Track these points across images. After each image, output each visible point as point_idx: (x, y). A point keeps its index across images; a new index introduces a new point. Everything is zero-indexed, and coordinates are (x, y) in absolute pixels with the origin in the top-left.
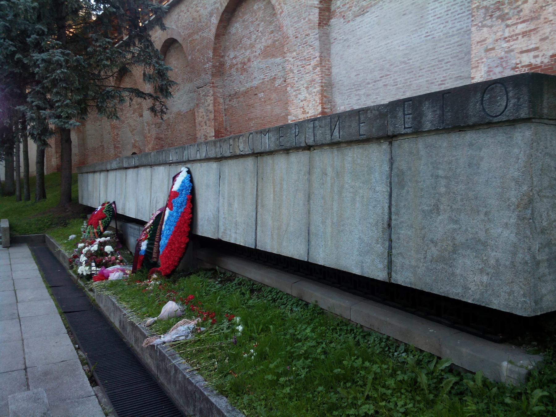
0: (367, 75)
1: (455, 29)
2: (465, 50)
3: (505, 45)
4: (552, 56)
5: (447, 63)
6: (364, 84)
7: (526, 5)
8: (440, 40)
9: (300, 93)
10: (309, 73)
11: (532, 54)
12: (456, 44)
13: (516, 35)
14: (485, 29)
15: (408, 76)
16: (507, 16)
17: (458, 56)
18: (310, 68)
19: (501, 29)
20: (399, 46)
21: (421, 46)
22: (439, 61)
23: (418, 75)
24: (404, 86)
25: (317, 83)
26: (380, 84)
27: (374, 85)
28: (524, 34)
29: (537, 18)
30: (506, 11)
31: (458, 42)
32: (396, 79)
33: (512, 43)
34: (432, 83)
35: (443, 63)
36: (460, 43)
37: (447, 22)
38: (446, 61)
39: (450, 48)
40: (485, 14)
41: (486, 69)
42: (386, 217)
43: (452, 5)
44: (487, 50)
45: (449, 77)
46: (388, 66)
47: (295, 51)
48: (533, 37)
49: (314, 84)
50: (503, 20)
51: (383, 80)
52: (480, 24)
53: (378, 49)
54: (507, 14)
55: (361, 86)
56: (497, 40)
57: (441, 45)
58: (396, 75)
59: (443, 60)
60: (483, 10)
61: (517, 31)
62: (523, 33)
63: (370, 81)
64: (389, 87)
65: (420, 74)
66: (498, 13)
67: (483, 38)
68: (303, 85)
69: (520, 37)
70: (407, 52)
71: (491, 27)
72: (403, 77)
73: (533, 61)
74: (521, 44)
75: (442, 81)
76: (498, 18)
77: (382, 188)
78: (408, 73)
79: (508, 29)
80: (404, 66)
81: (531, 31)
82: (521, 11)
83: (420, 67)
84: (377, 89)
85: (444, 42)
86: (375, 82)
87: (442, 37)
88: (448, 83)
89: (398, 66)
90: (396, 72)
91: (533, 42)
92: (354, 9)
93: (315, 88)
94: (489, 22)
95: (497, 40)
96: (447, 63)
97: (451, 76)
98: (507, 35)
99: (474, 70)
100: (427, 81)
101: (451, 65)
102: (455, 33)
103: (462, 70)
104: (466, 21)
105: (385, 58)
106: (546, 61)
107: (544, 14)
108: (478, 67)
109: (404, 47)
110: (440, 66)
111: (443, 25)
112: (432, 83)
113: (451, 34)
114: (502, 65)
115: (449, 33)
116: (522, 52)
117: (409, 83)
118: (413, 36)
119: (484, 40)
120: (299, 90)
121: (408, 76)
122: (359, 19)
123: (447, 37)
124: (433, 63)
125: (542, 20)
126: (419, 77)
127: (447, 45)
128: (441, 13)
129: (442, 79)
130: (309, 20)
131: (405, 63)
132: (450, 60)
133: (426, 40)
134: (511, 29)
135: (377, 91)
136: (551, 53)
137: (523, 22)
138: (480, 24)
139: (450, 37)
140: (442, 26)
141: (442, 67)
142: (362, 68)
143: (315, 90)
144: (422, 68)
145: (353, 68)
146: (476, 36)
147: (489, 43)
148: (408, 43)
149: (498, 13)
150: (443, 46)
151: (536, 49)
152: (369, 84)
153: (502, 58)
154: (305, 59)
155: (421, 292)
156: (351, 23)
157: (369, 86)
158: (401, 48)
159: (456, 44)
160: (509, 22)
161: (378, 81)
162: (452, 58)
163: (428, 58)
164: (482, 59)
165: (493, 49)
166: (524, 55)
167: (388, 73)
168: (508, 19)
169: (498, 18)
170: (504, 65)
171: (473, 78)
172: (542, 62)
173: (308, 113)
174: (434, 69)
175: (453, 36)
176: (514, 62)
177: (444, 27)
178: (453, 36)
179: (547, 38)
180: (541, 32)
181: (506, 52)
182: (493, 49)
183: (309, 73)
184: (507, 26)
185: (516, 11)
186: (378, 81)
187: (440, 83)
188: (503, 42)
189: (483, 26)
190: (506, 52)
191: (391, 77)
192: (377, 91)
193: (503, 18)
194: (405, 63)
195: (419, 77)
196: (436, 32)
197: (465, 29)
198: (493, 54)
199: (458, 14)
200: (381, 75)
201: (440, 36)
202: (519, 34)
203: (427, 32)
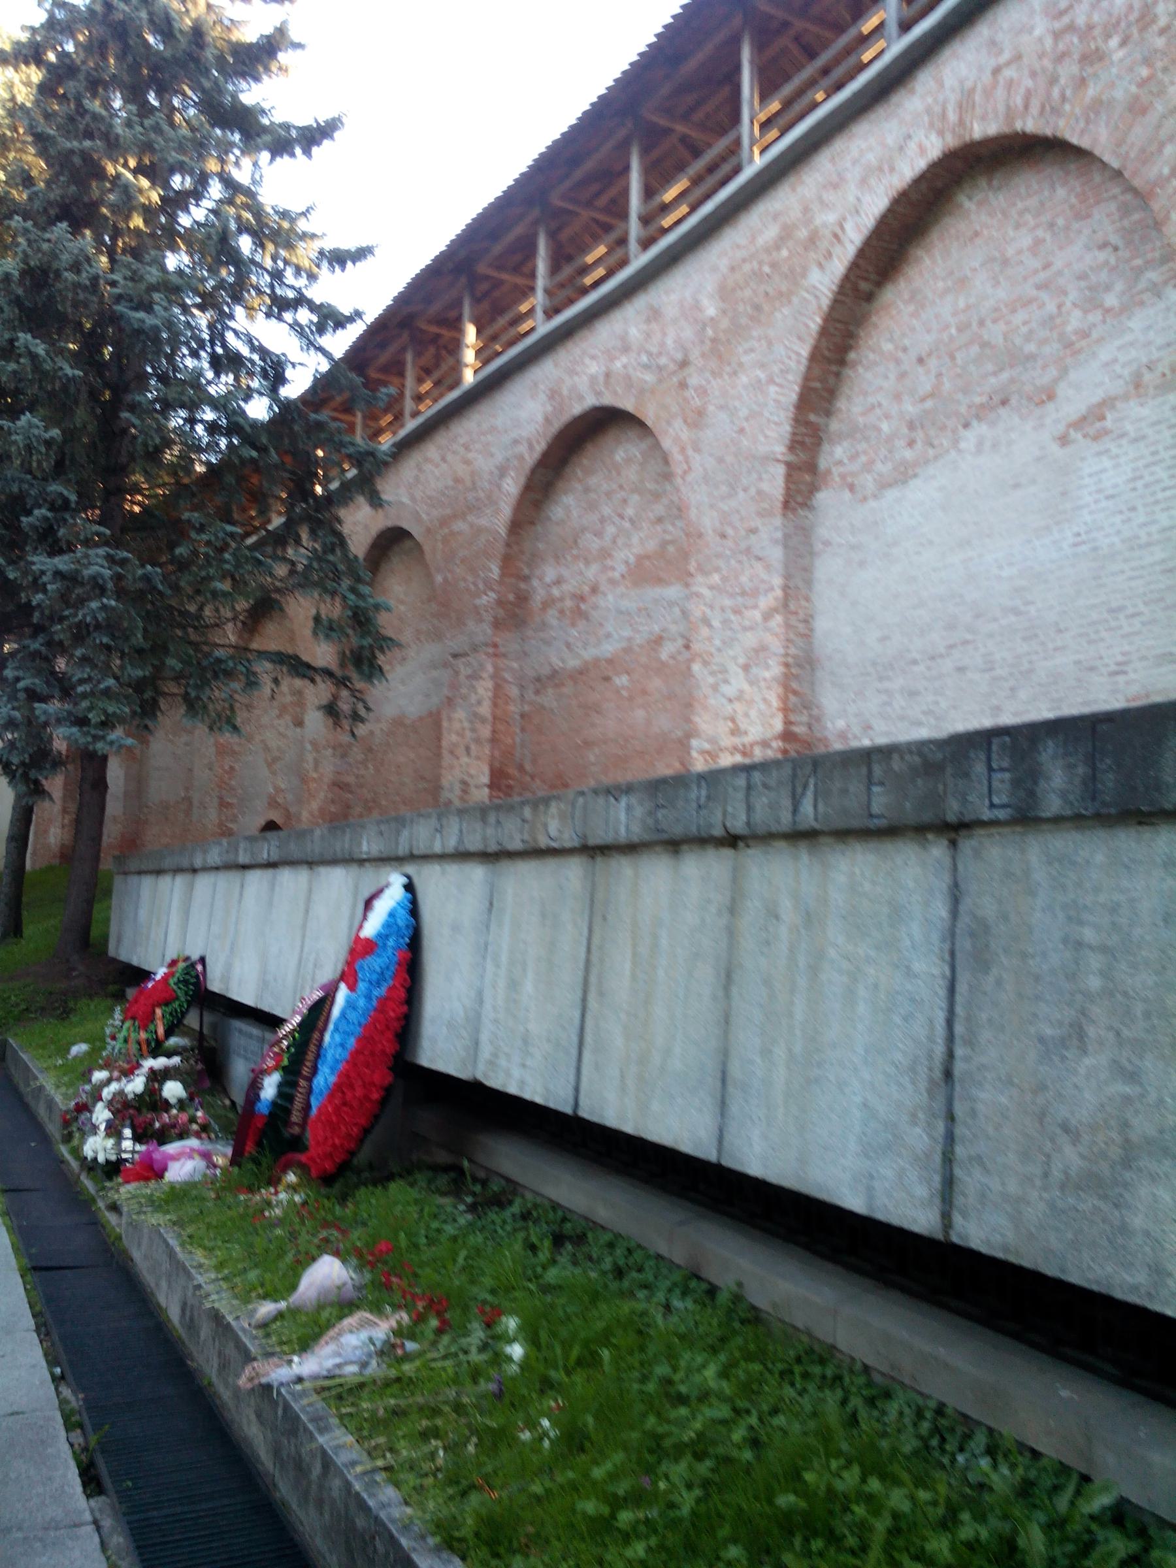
1: (1154, 529)
5: (1133, 615)
9: (726, 682)
17: (1162, 599)
18: (757, 615)
20: (1001, 567)
22: (1111, 611)
23: (1051, 646)
26: (947, 665)
31: (1163, 561)
35: (1121, 616)
37: (1133, 509)
38: (1131, 610)
39: (1141, 577)
42: (940, 1050)
43: (1147, 466)
47: (717, 569)
59: (1121, 609)
63: (918, 657)
75: (1118, 664)
77: (929, 968)
80: (1013, 618)
83: (1057, 624)
85: (1126, 561)
90: (991, 635)
92: (879, 467)
96: (1133, 615)
100: (1078, 663)
101: (1143, 624)
110: (1113, 624)
112: (1092, 669)
115: (1138, 537)
122: (891, 494)
123: (1132, 549)
124: (1095, 616)
126: (1056, 649)
127: (1133, 569)
128: (1116, 486)
129: (1120, 658)
130: (760, 492)
131: (1016, 612)
132: (1142, 608)
139: (1140, 547)
140: (1118, 519)
141: (1120, 627)
150: (1123, 572)
152: (915, 662)
154: (743, 593)
155: (1035, 1277)
156: (872, 504)
157: (916, 668)
158: (1005, 573)
159: (1158, 568)
161: (941, 656)
162: (1146, 604)
175: (1149, 544)
177: (1124, 522)
178: (1149, 544)
186: (941, 656)
187: (1113, 668)
194: (1016, 612)
195: (1056, 649)
199: (1164, 490)
201: (1112, 545)
203: (1079, 535)
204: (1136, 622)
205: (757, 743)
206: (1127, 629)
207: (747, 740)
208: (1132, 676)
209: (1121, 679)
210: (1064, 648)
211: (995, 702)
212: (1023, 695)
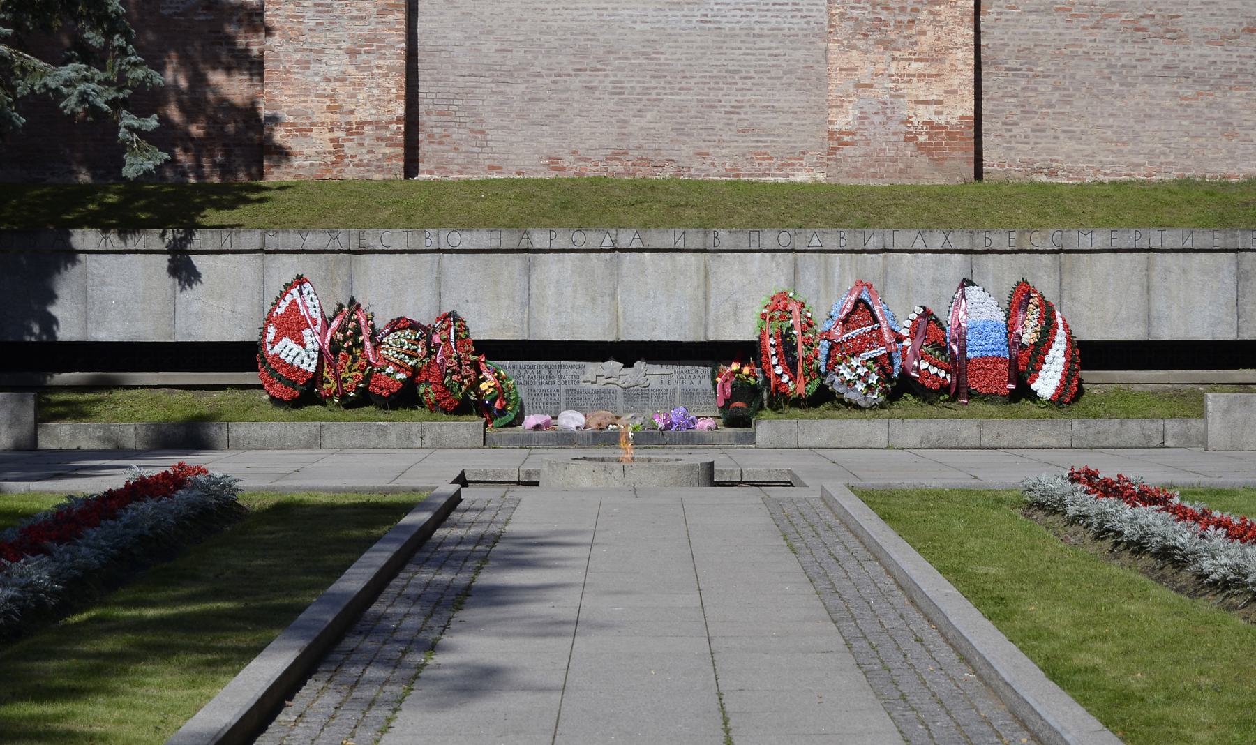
0: (536, 58)
1: (765, 26)
2: (784, 64)
3: (891, 85)
4: (961, 117)
5: (746, 78)
6: (524, 73)
7: (923, 38)
8: (732, 36)
9: (318, 61)
10: (362, 18)
11: (933, 108)
12: (767, 52)
13: (908, 75)
14: (854, 53)
15: (654, 83)
16: (894, 45)
19: (883, 61)
20: (635, 22)
21: (688, 35)
23: (678, 86)
24: (640, 100)
25: (392, 47)
26: (576, 83)
27: (553, 82)
28: (921, 77)
29: (940, 60)
30: (892, 37)
31: (770, 48)
32: (621, 82)
33: (902, 85)
34: (711, 107)
35: (737, 76)
36: (775, 52)
37: (751, 10)
38: (744, 74)
40: (855, 30)
41: (857, 113)
44: (859, 86)
45: (748, 104)
46: (601, 51)
48: (934, 86)
49: (379, 48)
50: (886, 48)
51: (584, 76)
52: (845, 42)
53: (575, 12)
54: (894, 41)
55: (512, 76)
56: (877, 75)
57: (734, 45)
58: (619, 74)
59: (738, 71)
60: (851, 23)
61: (910, 71)
62: (920, 76)
63: (544, 72)
64: (597, 94)
65: (684, 85)
66: (877, 35)
67: (850, 65)
68: (336, 41)
69: (915, 80)
70: (653, 37)
71: (866, 52)
72: (639, 82)
73: (934, 118)
74: (916, 90)
76: (877, 42)
78: (653, 77)
79: (895, 63)
81: (930, 76)
82: (916, 43)
83: (683, 71)
84: (566, 90)
85: (742, 42)
86: (560, 76)
87: (737, 32)
88: (746, 113)
89: (627, 58)
90: (622, 69)
91: (936, 93)
93: (383, 57)
94: (862, 44)
95: (877, 75)
96: (746, 78)
97: (752, 102)
98: (893, 71)
99: (834, 110)
102: (766, 32)
103: (777, 97)
104: (790, 20)
105: (594, 34)
106: (953, 122)
107: (949, 59)
108: (841, 106)
109: (647, 27)
110: (730, 80)
111: (743, 13)
112: (711, 107)
113: (757, 32)
114: (884, 113)
116: (917, 102)
117: (654, 96)
118: (670, 13)
119: (855, 69)
120: (322, 51)
121: (654, 83)
123: (748, 35)
124: (715, 72)
125: (947, 65)
132: (752, 74)
133: (701, 28)
134: (901, 65)
135: (563, 96)
136: (960, 113)
137: (920, 60)
138: (845, 42)
140: (739, 13)
142: (521, 38)
143: (381, 63)
144: (688, 74)
145: (489, 32)
146: (838, 59)
147: (864, 74)
148: (660, 21)
149: (877, 35)
151: (940, 102)
152: (540, 76)
153: (885, 103)
157: (539, 80)
158: (638, 26)
160: (897, 54)
161: (569, 75)
163: (704, 61)
164: (848, 96)
165: (871, 86)
166: (921, 106)
167: (599, 66)
168: (895, 49)
169: (877, 42)
170: (888, 111)
171: (832, 122)
172: (947, 123)
173: (352, 112)
174: (717, 83)
175: (760, 36)
176: (905, 113)
178: (760, 36)
179: (955, 92)
180: (947, 82)
181: (891, 96)
182: (871, 86)
183: (362, 18)
184: (894, 59)
185: (908, 41)
186: (569, 75)
187: (728, 109)
188: (888, 80)
189: (854, 47)
190: (891, 96)
191: (606, 76)
192: (563, 96)
193: (887, 45)
196: (725, 20)
197: (786, 32)
198: (868, 93)
200: (579, 67)
201: (733, 29)
202: (914, 76)
204: (749, 82)
205: (370, 123)
206: (740, 86)
207: (357, 118)
208: (743, 116)
209: (735, 117)
210: (689, 89)
211: (621, 116)
212: (649, 116)
